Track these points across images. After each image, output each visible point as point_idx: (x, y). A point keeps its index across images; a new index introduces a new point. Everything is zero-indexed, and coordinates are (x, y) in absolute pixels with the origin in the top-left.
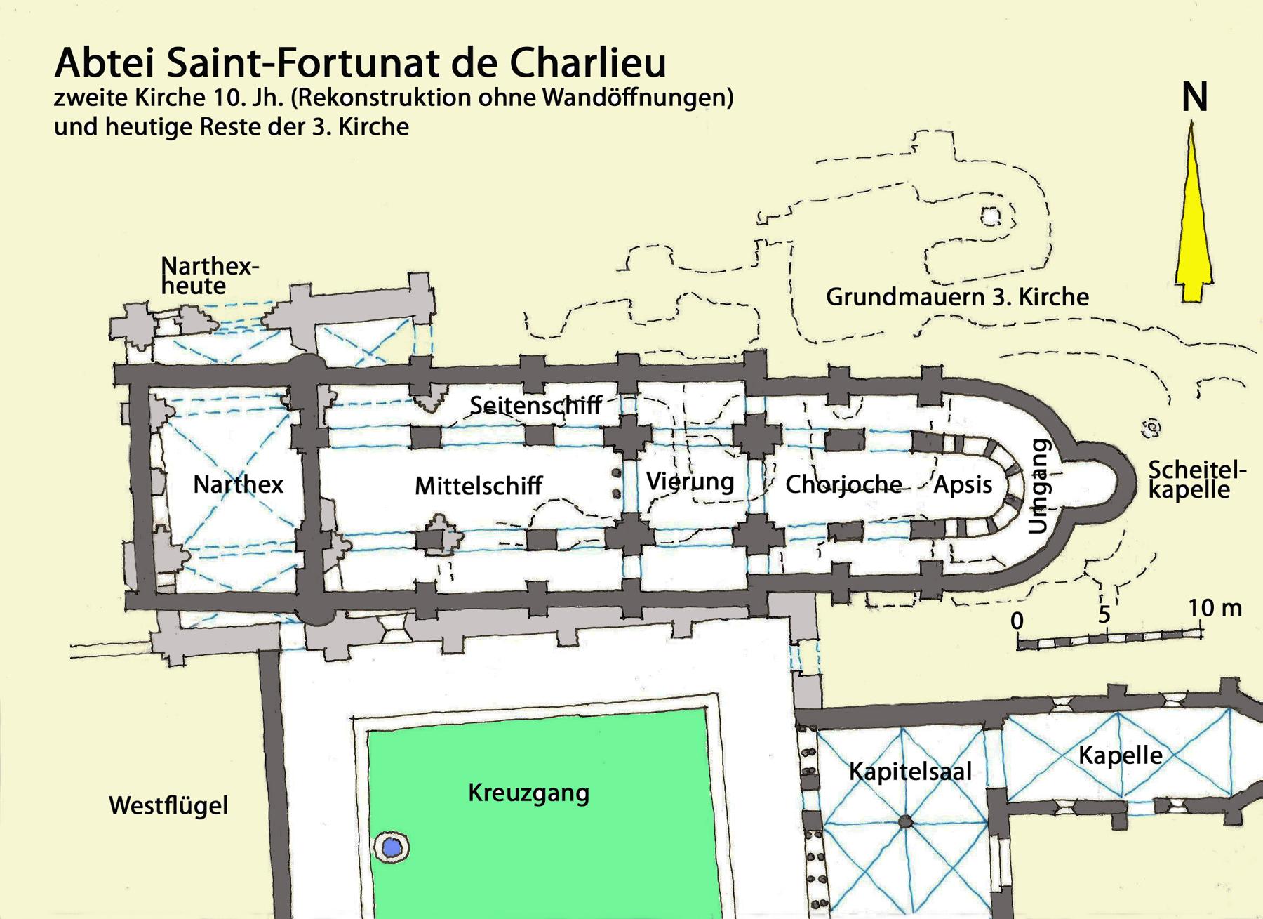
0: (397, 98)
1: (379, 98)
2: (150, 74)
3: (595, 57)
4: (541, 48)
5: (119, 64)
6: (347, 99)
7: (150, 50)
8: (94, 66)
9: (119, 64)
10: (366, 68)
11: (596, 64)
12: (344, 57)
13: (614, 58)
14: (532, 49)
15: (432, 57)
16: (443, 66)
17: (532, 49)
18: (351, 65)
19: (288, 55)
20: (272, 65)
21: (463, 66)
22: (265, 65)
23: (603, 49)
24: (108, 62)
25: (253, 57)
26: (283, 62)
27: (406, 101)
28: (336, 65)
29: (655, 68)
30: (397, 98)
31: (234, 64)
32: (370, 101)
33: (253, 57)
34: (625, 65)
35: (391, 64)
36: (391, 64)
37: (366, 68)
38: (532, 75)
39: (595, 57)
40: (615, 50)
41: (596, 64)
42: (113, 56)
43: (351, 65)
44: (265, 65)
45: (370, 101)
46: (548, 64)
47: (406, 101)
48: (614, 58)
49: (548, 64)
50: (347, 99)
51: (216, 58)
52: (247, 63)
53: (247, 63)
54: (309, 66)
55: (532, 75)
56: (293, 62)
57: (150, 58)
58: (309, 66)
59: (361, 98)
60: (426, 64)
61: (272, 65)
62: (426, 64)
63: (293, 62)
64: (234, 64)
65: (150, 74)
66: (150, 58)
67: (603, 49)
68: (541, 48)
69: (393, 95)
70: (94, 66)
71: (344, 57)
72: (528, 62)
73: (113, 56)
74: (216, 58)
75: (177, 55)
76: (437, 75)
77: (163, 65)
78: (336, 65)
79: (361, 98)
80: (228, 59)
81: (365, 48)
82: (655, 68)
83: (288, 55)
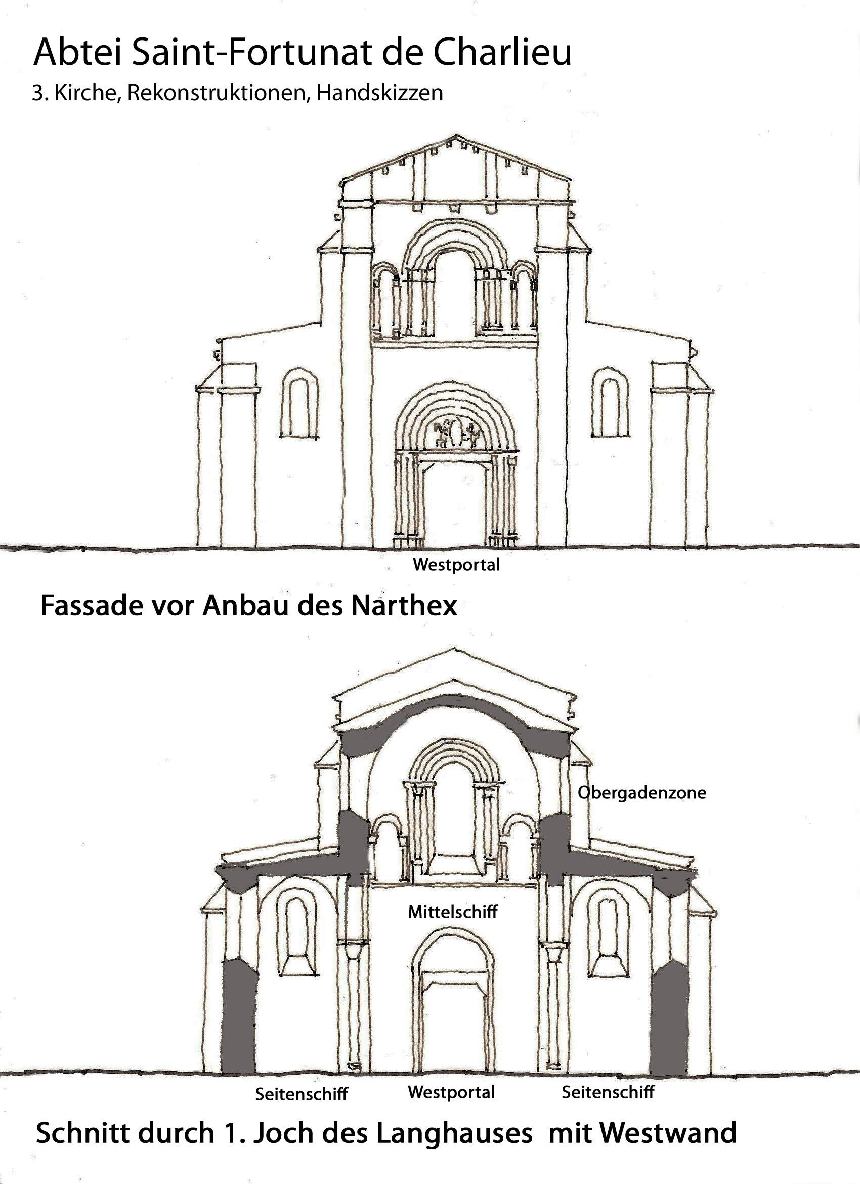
0: (215, 93)
1: (199, 93)
2: (118, 63)
3: (509, 47)
4: (461, 38)
5: (91, 53)
6: (170, 94)
7: (118, 40)
8: (69, 55)
9: (91, 53)
10: (307, 57)
11: (510, 54)
12: (288, 46)
13: (526, 47)
14: (453, 39)
15: (365, 46)
16: (375, 55)
17: (453, 39)
18: (294, 53)
19: (238, 45)
20: (225, 54)
21: (392, 55)
22: (218, 54)
23: (516, 38)
24: (81, 51)
25: (208, 46)
26: (233, 51)
27: (222, 96)
28: (281, 54)
29: (562, 57)
30: (215, 93)
31: (191, 53)
32: (191, 96)
33: (208, 46)
34: (535, 54)
35: (330, 53)
36: (330, 53)
37: (307, 57)
38: (453, 63)
39: (509, 47)
40: (526, 40)
41: (510, 54)
42: (86, 46)
43: (294, 53)
44: (218, 54)
45: (191, 96)
46: (468, 53)
47: (222, 96)
48: (526, 47)
49: (468, 53)
50: (170, 94)
51: (175, 47)
52: (203, 52)
53: (203, 52)
54: (257, 55)
55: (453, 63)
56: (243, 51)
57: (118, 47)
58: (257, 55)
59: (183, 93)
60: (360, 52)
61: (225, 54)
62: (360, 52)
63: (243, 51)
64: (191, 53)
65: (118, 63)
66: (118, 47)
67: (516, 38)
68: (461, 38)
69: (211, 91)
70: (69, 55)
71: (288, 46)
72: (449, 51)
73: (86, 46)
74: (175, 47)
75: (140, 44)
76: (370, 64)
77: (129, 54)
78: (281, 54)
79: (183, 93)
80: (185, 49)
81: (306, 39)
82: (562, 57)
83: (238, 45)
